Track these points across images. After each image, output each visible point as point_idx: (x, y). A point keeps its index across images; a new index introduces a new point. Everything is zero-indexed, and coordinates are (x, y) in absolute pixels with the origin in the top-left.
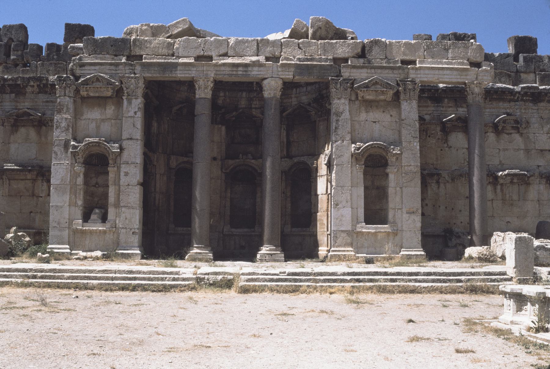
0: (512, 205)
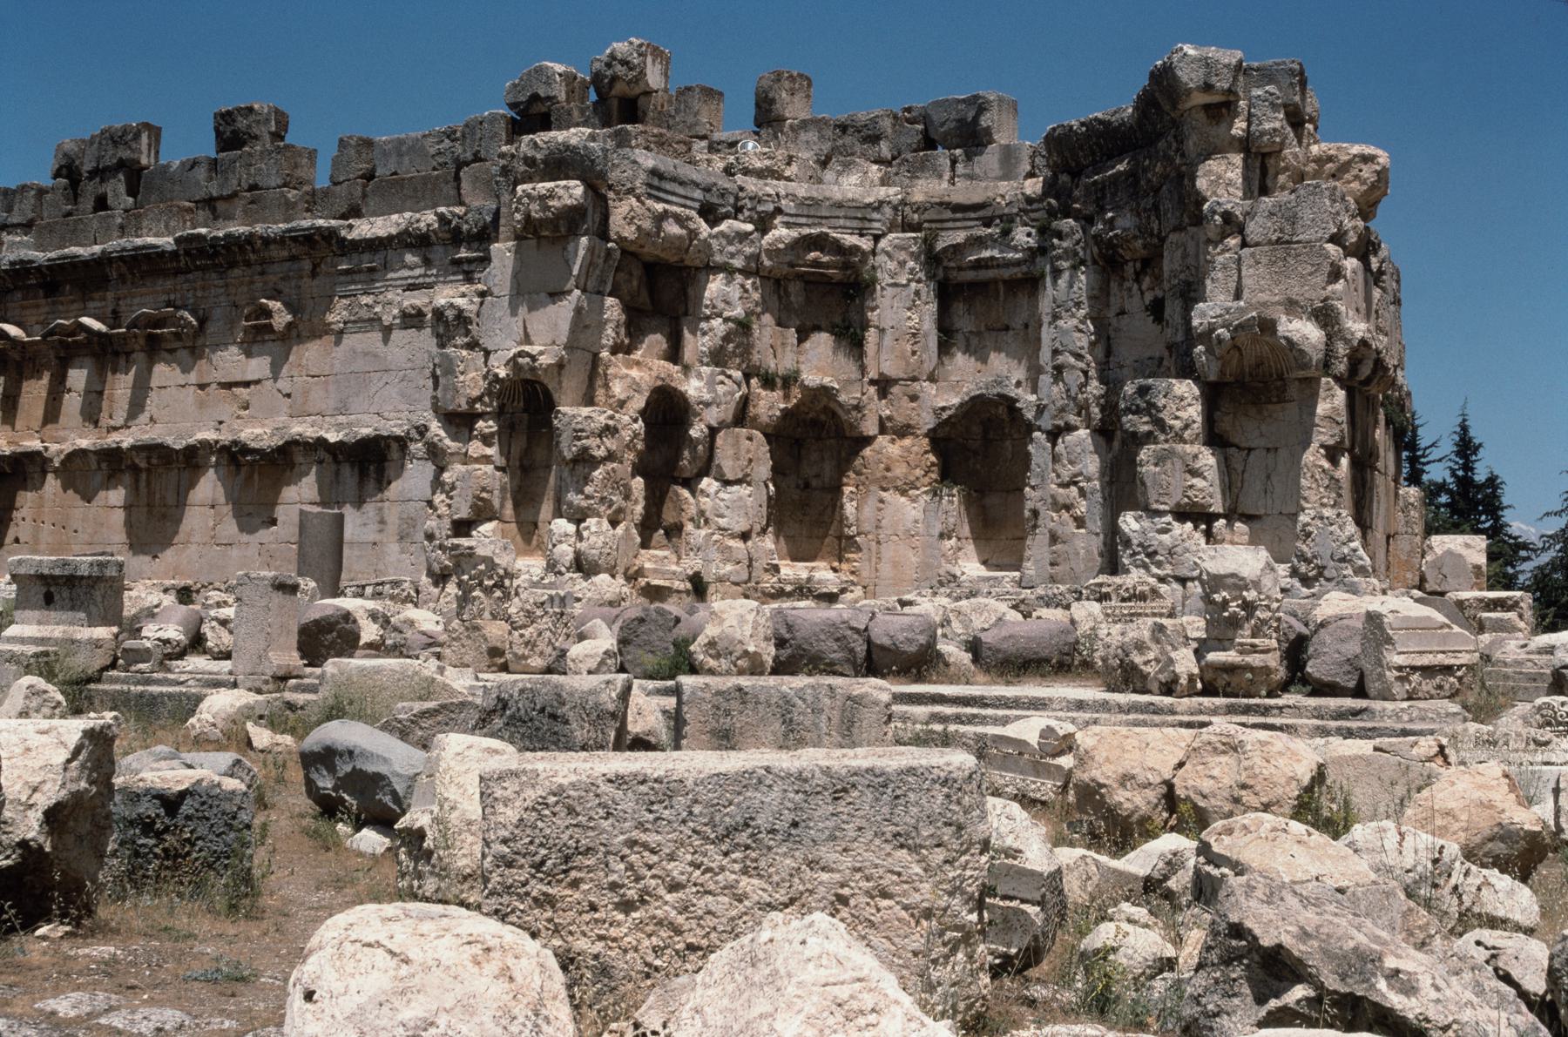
0: (164, 516)
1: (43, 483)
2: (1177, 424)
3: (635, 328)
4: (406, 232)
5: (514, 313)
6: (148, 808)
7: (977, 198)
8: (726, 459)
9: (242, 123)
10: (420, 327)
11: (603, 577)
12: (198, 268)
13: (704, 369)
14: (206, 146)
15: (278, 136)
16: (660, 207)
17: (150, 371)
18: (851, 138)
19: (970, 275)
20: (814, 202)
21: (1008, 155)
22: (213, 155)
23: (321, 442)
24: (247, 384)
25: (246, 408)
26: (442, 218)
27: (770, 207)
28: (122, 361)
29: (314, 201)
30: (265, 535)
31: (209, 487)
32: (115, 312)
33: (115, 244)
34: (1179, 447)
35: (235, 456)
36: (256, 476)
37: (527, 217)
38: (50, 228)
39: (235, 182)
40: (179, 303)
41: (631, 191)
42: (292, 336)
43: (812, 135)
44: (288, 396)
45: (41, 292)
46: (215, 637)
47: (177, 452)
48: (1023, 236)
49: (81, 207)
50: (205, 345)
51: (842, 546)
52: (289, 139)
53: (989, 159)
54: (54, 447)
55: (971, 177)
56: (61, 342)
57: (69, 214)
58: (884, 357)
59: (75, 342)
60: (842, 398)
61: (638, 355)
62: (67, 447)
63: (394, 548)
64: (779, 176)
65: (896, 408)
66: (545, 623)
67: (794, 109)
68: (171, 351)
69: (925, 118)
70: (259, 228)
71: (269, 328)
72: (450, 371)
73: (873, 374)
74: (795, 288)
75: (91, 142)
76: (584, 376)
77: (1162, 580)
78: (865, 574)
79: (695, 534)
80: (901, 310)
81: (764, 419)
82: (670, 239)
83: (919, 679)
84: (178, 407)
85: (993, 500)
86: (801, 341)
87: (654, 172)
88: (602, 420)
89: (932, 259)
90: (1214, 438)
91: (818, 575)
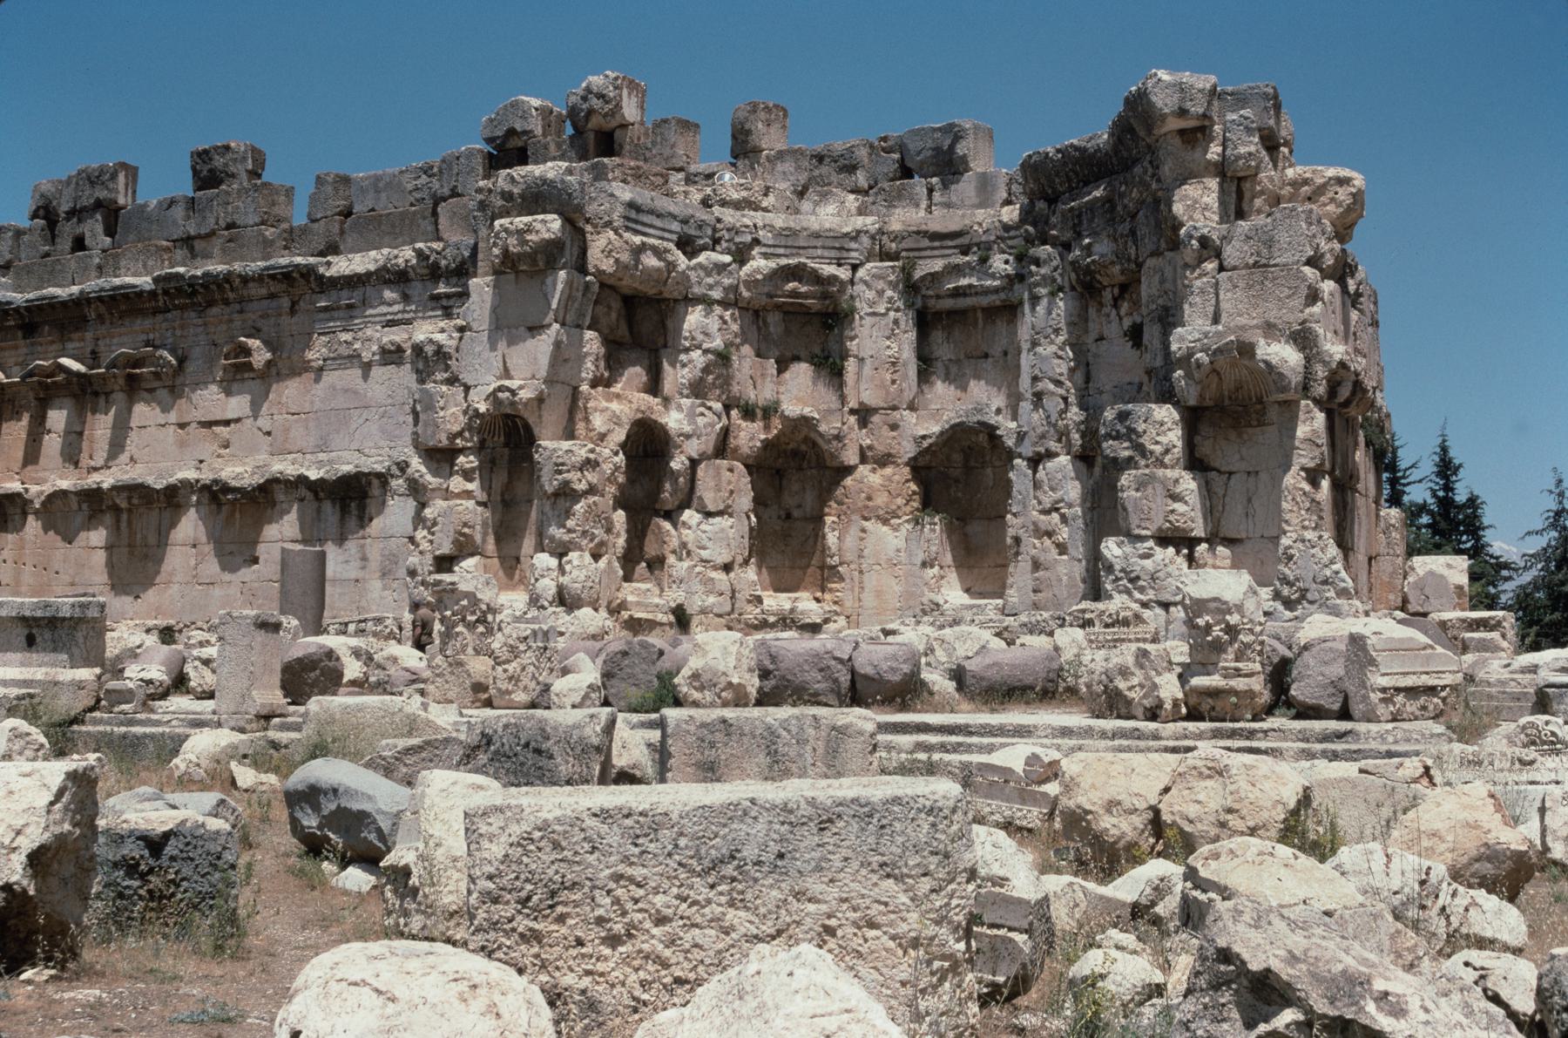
0: (146, 556)
1: (24, 524)
2: (1158, 449)
3: (614, 361)
4: (384, 268)
5: (493, 348)
6: (133, 850)
7: (953, 227)
8: (707, 492)
9: (219, 162)
10: (399, 363)
11: (586, 612)
12: (176, 307)
13: (686, 402)
14: (184, 186)
15: (254, 174)
16: (637, 239)
17: (130, 411)
18: (828, 168)
19: (948, 304)
20: (792, 233)
21: (985, 183)
22: (191, 194)
23: (302, 480)
24: (227, 423)
25: (226, 447)
26: (420, 254)
27: (748, 238)
28: (102, 400)
29: (292, 239)
30: (247, 573)
31: (190, 526)
32: (93, 352)
33: (93, 284)
34: (1160, 472)
35: (215, 495)
36: (237, 515)
37: (506, 252)
38: (28, 270)
39: (213, 221)
40: (157, 342)
41: (608, 224)
42: (271, 374)
43: (787, 166)
44: (269, 434)
45: (20, 334)
46: (198, 677)
47: (158, 491)
48: (1001, 263)
49: (59, 247)
50: (184, 385)
51: (826, 576)
52: (267, 176)
53: (966, 187)
54: (34, 489)
55: (948, 205)
56: (40, 383)
57: (47, 255)
58: (863, 386)
59: (54, 383)
60: (823, 428)
61: (617, 388)
62: (48, 489)
63: (376, 584)
64: (756, 207)
65: (877, 437)
66: (528, 658)
67: (770, 139)
68: (151, 391)
69: (901, 147)
70: (237, 267)
71: (248, 367)
72: (430, 406)
73: (853, 403)
74: (774, 319)
75: (68, 182)
76: (563, 409)
77: (1145, 605)
78: (848, 604)
79: (678, 567)
80: (880, 339)
81: (745, 450)
82: (649, 273)
83: (904, 708)
84: (157, 447)
85: (975, 528)
86: (780, 371)
87: (631, 205)
88: (583, 453)
89: (911, 288)
90: (1195, 463)
91: (801, 606)
